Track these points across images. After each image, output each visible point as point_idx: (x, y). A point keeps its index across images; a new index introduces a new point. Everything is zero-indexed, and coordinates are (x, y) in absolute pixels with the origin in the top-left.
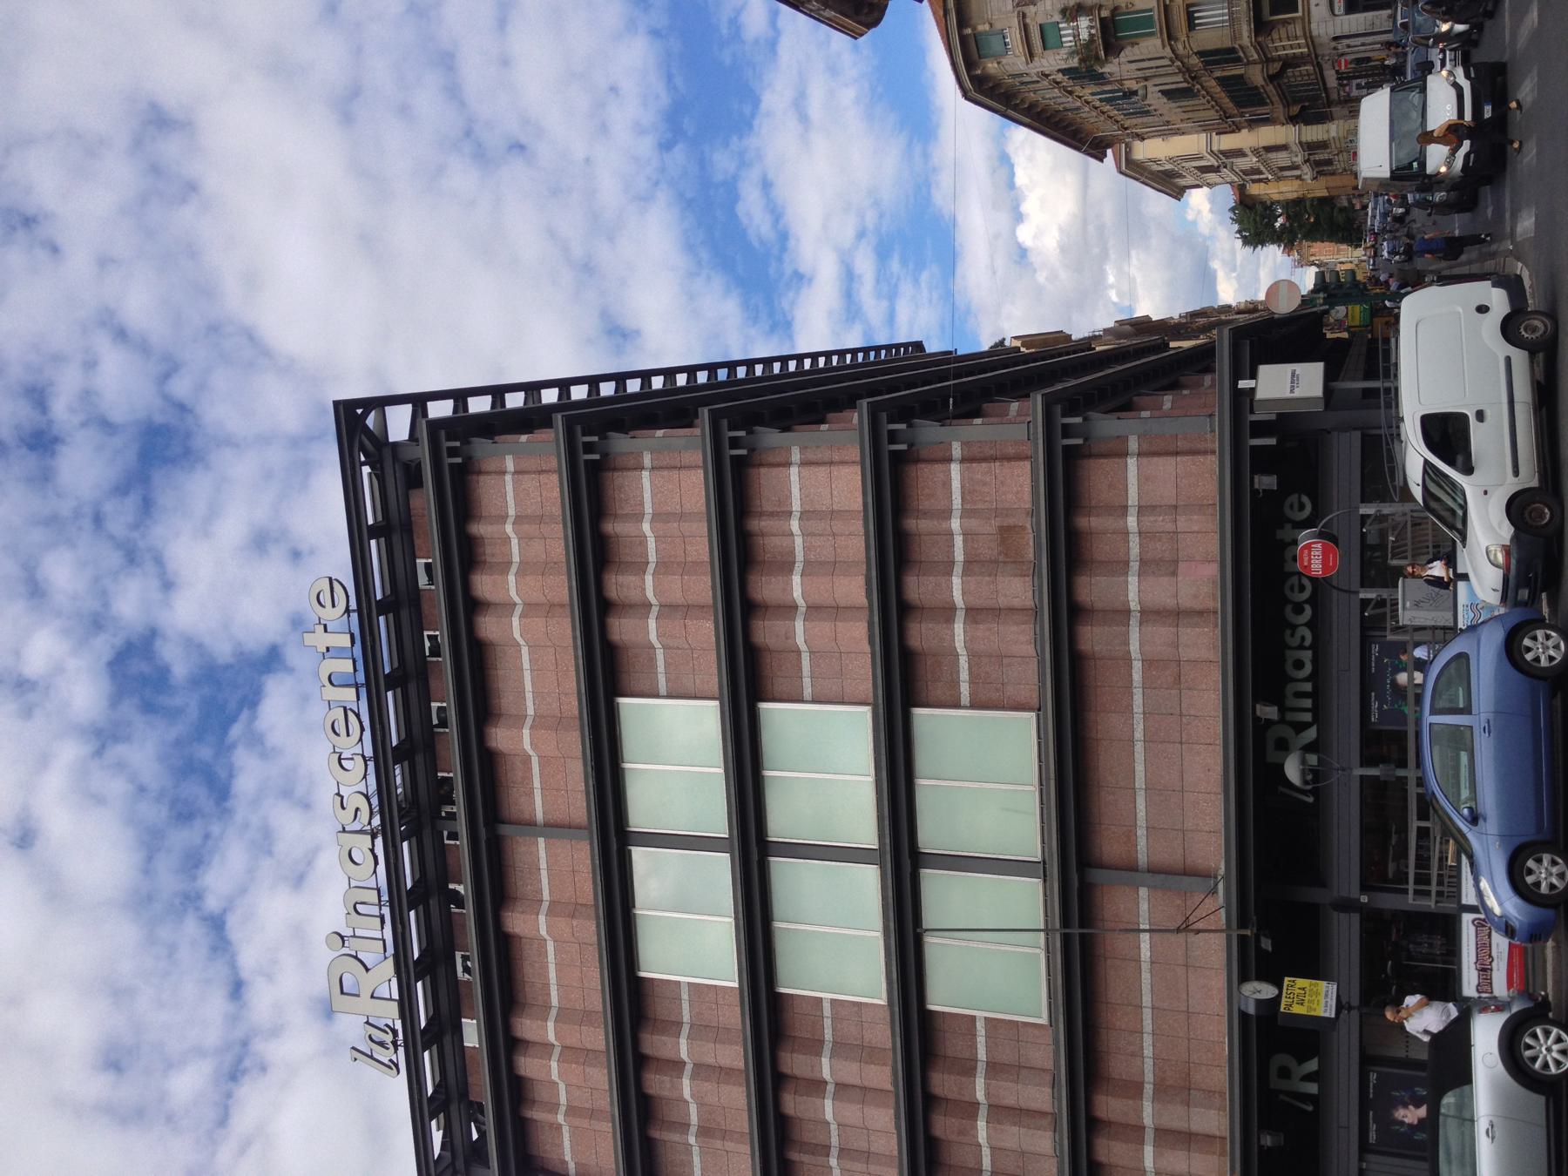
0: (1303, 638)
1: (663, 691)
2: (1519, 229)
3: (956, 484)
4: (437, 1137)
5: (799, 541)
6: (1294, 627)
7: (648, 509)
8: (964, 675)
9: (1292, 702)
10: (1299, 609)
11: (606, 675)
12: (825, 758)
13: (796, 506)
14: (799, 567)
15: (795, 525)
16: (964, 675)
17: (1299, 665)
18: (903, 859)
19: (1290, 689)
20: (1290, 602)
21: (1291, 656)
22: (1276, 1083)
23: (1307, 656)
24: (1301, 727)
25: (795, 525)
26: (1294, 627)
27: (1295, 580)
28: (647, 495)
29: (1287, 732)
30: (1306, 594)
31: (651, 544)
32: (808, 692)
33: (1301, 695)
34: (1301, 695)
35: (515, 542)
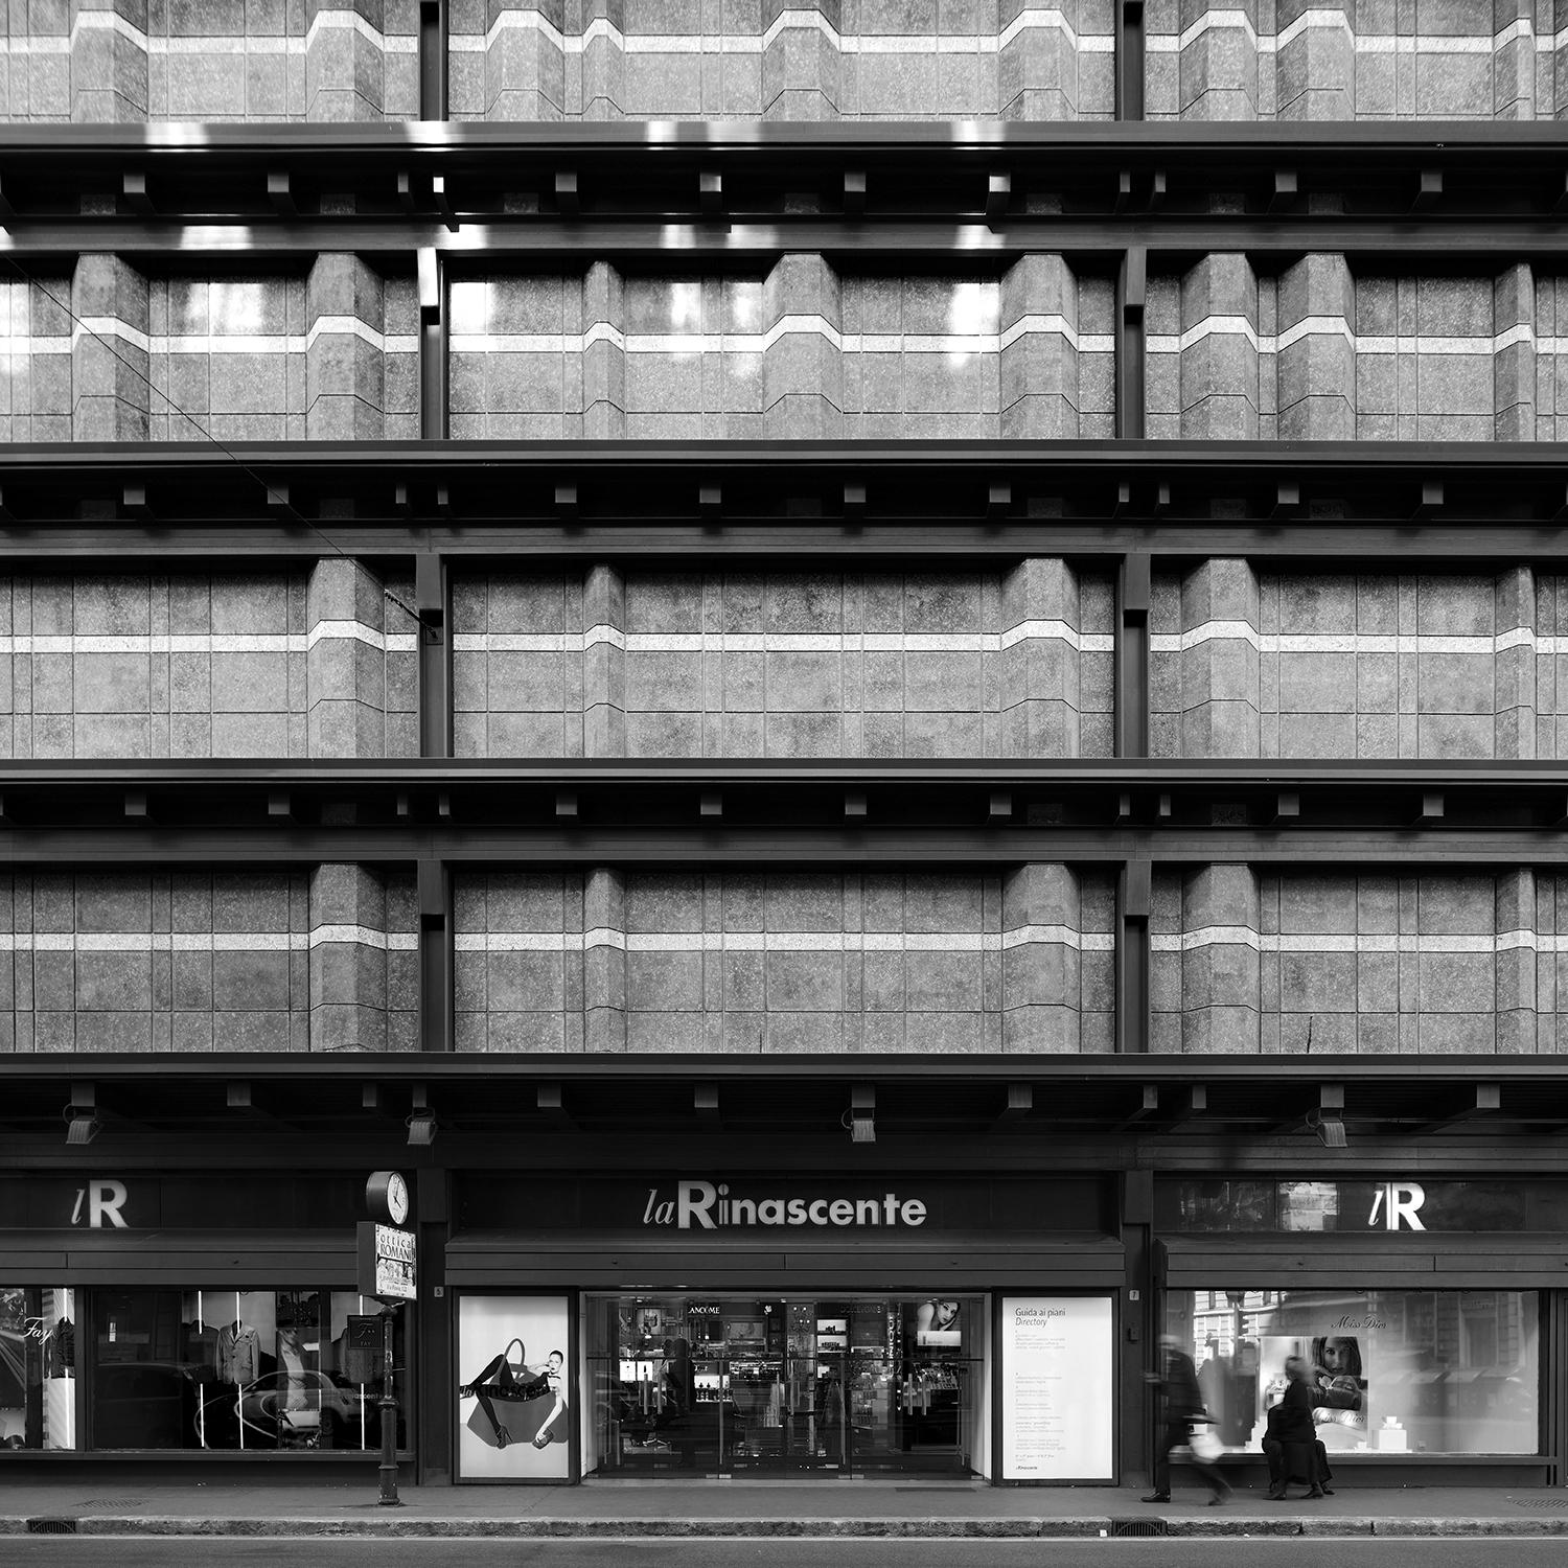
0: (798, 1207)
2: (1320, 1409)
6: (806, 1208)
9: (737, 1205)
10: (823, 1212)
17: (771, 1212)
19: (749, 1204)
20: (829, 1205)
21: (779, 1205)
23: (779, 1219)
24: (713, 1212)
26: (806, 1208)
27: (849, 1210)
30: (836, 1220)
33: (744, 1211)
34: (744, 1211)
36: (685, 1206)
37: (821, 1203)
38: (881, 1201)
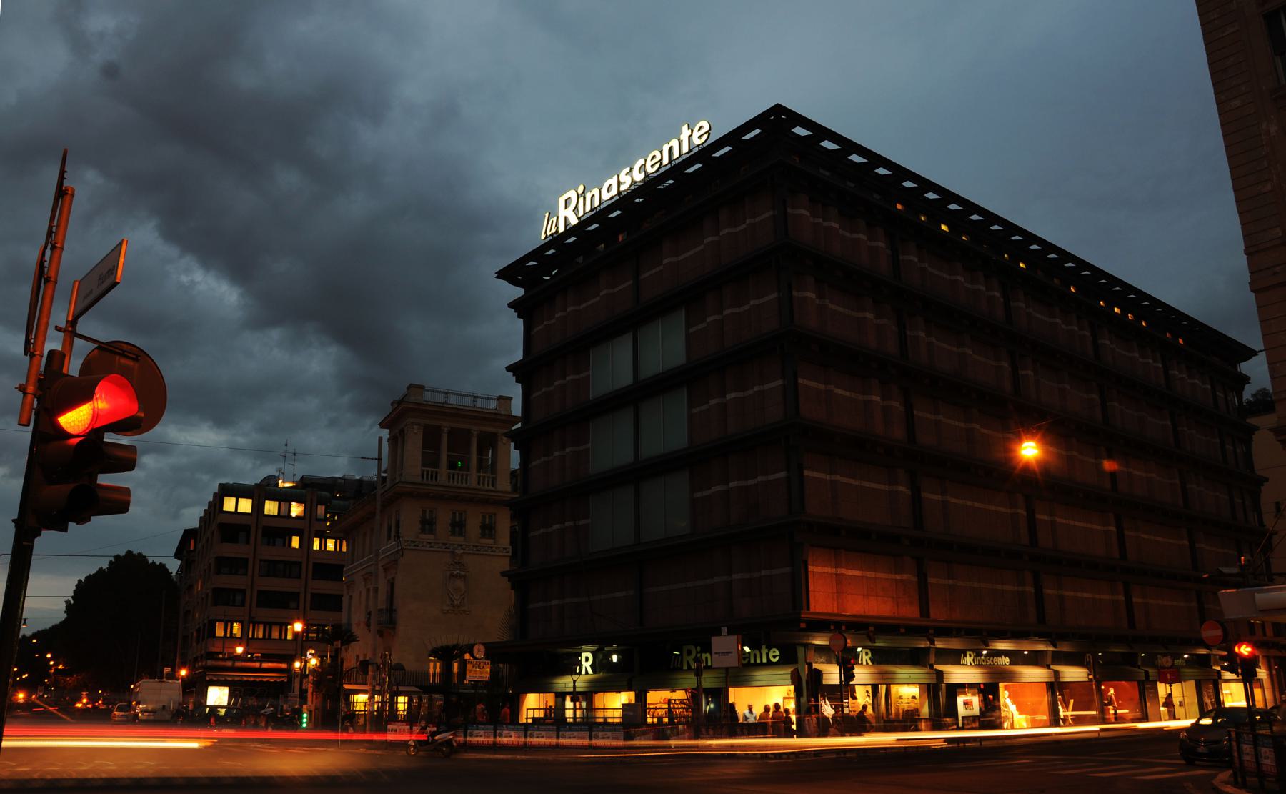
1: (691, 330)
3: (778, 475)
4: (532, 263)
5: (750, 392)
7: (762, 301)
8: (705, 493)
11: (688, 297)
12: (668, 427)
13: (767, 386)
14: (741, 395)
15: (756, 389)
16: (705, 493)
18: (638, 474)
22: (584, 655)
25: (756, 389)
28: (767, 298)
29: (694, 655)
31: (746, 307)
32: (694, 411)
35: (744, 226)
36: (563, 213)
37: (641, 161)
38: (677, 135)
